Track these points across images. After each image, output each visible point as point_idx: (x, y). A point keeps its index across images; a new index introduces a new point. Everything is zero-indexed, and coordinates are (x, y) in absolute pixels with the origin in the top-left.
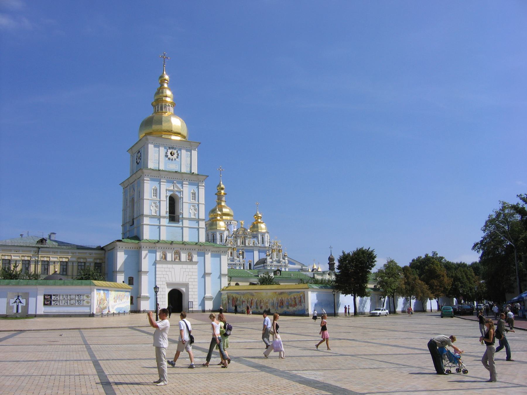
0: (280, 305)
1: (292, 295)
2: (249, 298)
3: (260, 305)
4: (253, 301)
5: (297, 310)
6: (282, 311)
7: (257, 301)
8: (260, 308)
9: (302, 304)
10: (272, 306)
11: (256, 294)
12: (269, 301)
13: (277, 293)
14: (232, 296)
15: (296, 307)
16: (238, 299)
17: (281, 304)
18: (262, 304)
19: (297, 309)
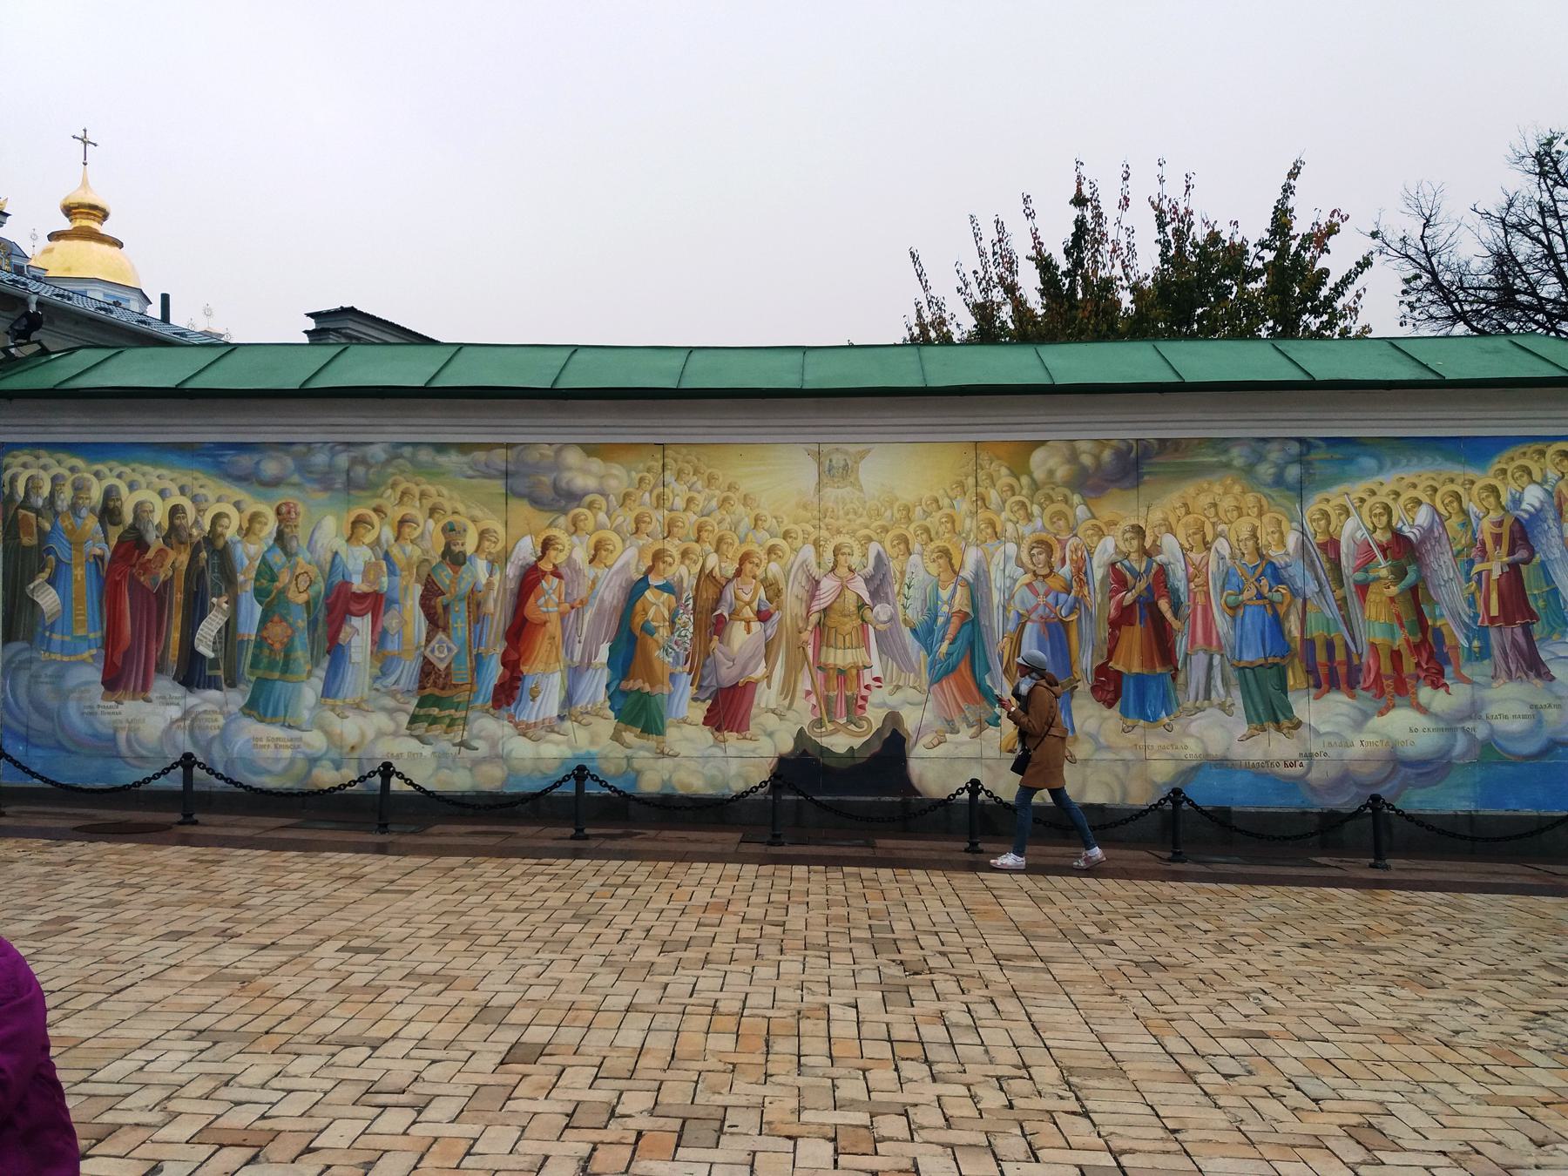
0: (1101, 670)
1: (1359, 489)
2: (470, 543)
3: (700, 662)
4: (549, 584)
5: (1461, 744)
6: (1162, 771)
7: (636, 590)
8: (699, 712)
9: (1544, 656)
10: (941, 673)
11: (618, 476)
12: (876, 594)
13: (1037, 456)
14: (108, 513)
15: (1425, 693)
16: (223, 557)
17: (1134, 636)
18: (742, 638)
19: (1450, 722)
